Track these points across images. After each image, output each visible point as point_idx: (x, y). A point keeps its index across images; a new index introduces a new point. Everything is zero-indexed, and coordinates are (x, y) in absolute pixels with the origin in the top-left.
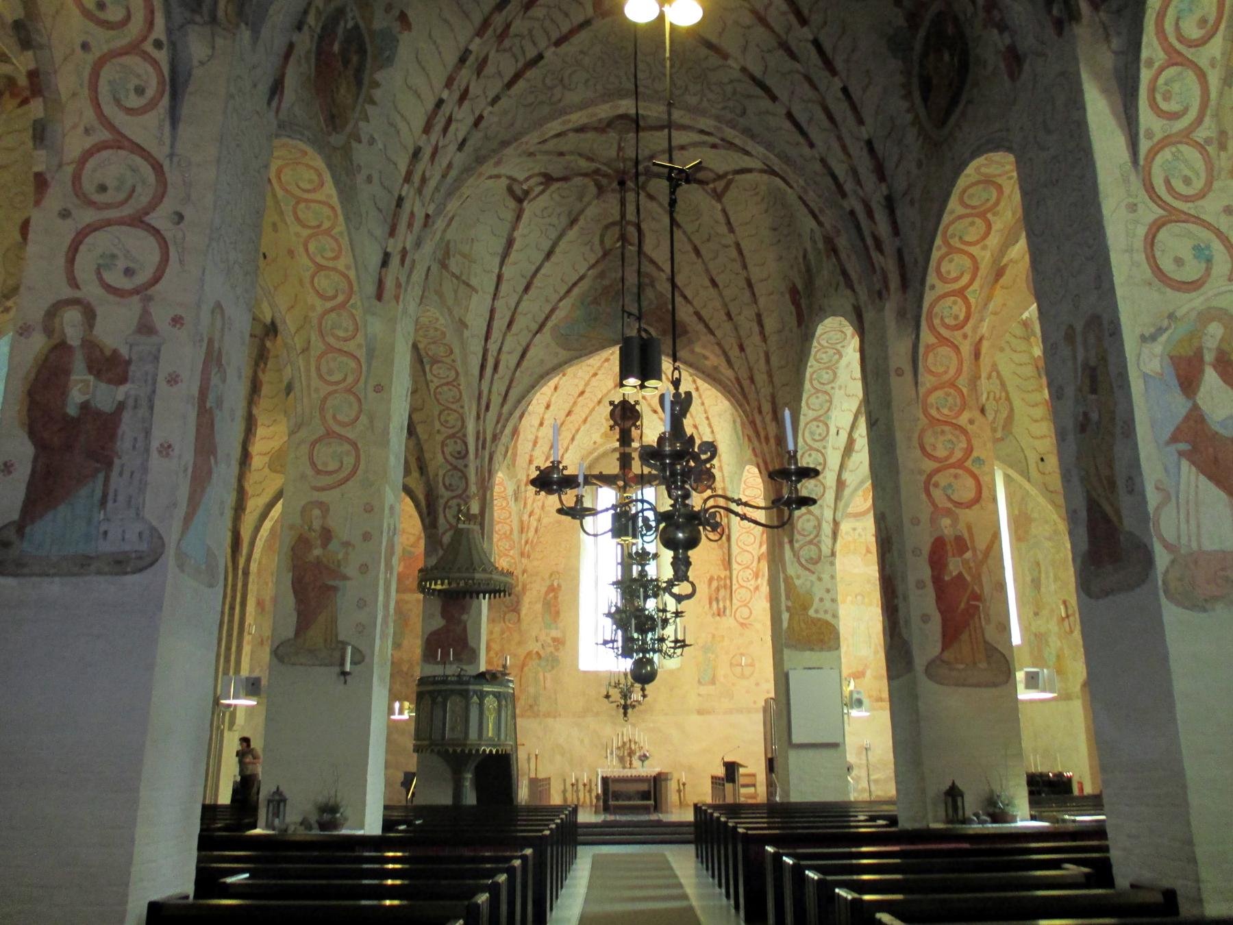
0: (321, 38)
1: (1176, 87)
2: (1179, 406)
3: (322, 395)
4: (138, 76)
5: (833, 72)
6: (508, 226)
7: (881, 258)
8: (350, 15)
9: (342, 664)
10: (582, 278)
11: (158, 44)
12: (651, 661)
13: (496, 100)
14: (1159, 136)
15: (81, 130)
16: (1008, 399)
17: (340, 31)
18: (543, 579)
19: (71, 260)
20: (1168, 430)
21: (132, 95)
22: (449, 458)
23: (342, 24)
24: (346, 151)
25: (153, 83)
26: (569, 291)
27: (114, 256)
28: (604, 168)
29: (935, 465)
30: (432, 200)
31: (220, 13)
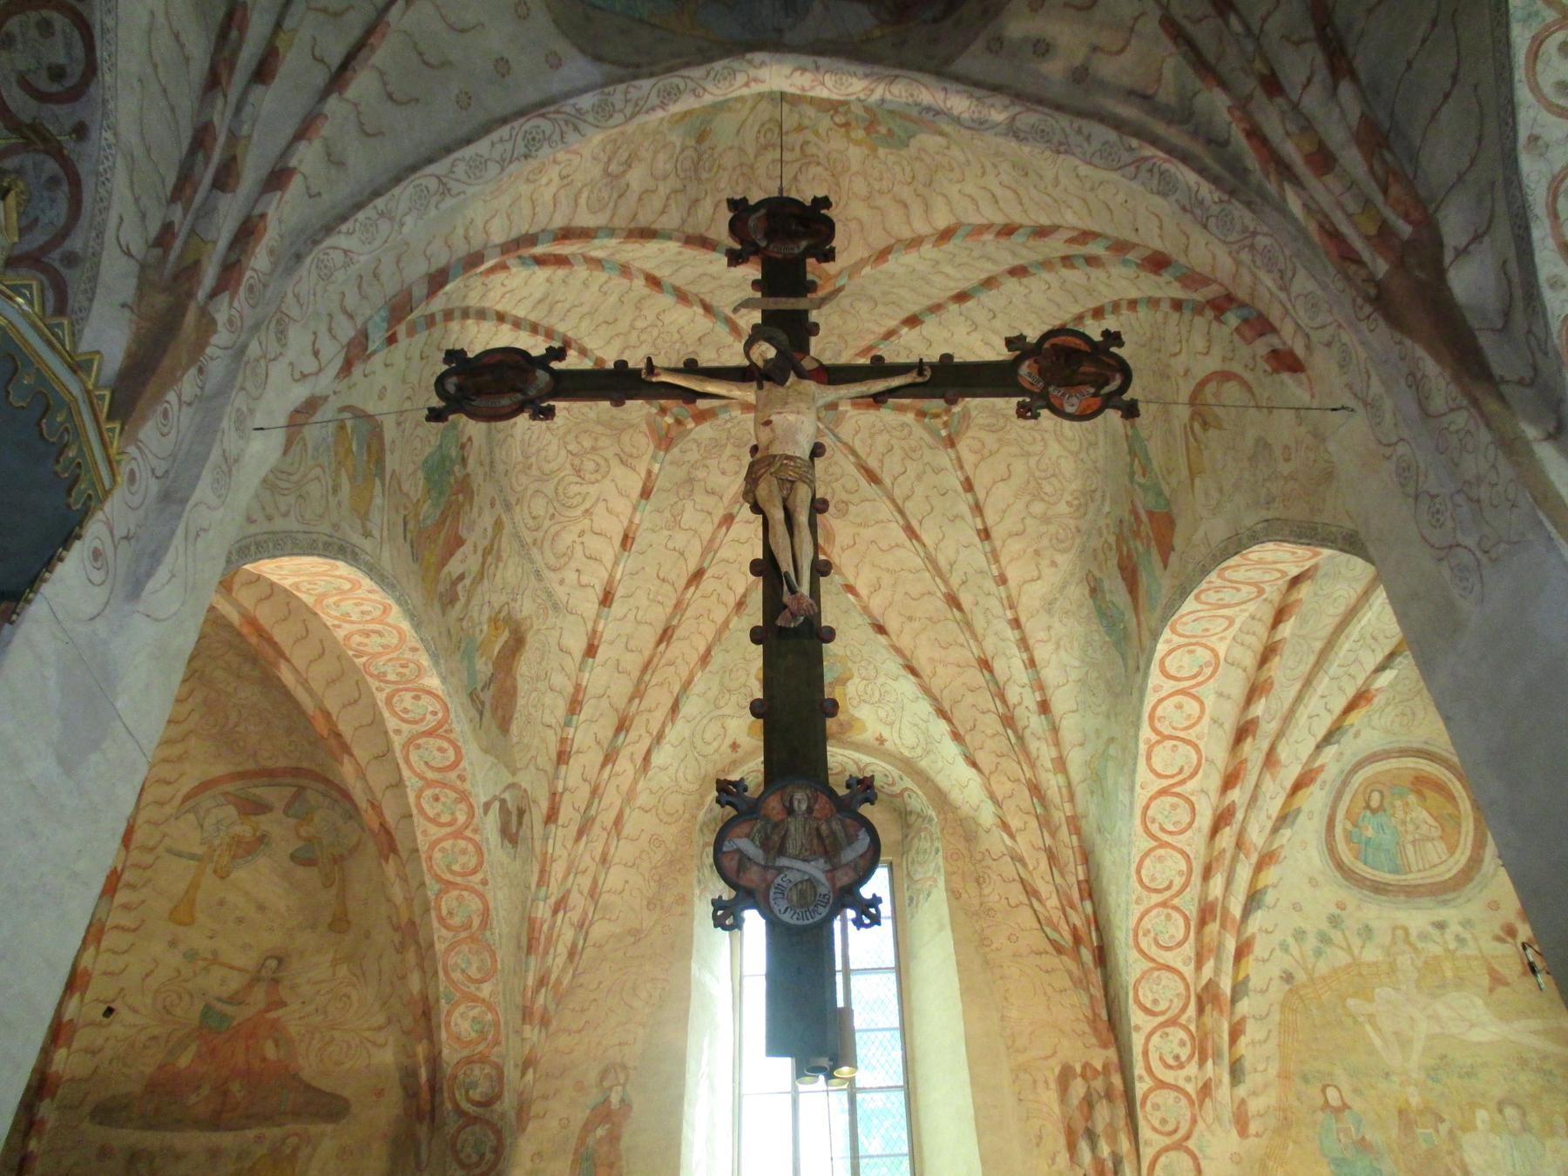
18: (580, 1087)
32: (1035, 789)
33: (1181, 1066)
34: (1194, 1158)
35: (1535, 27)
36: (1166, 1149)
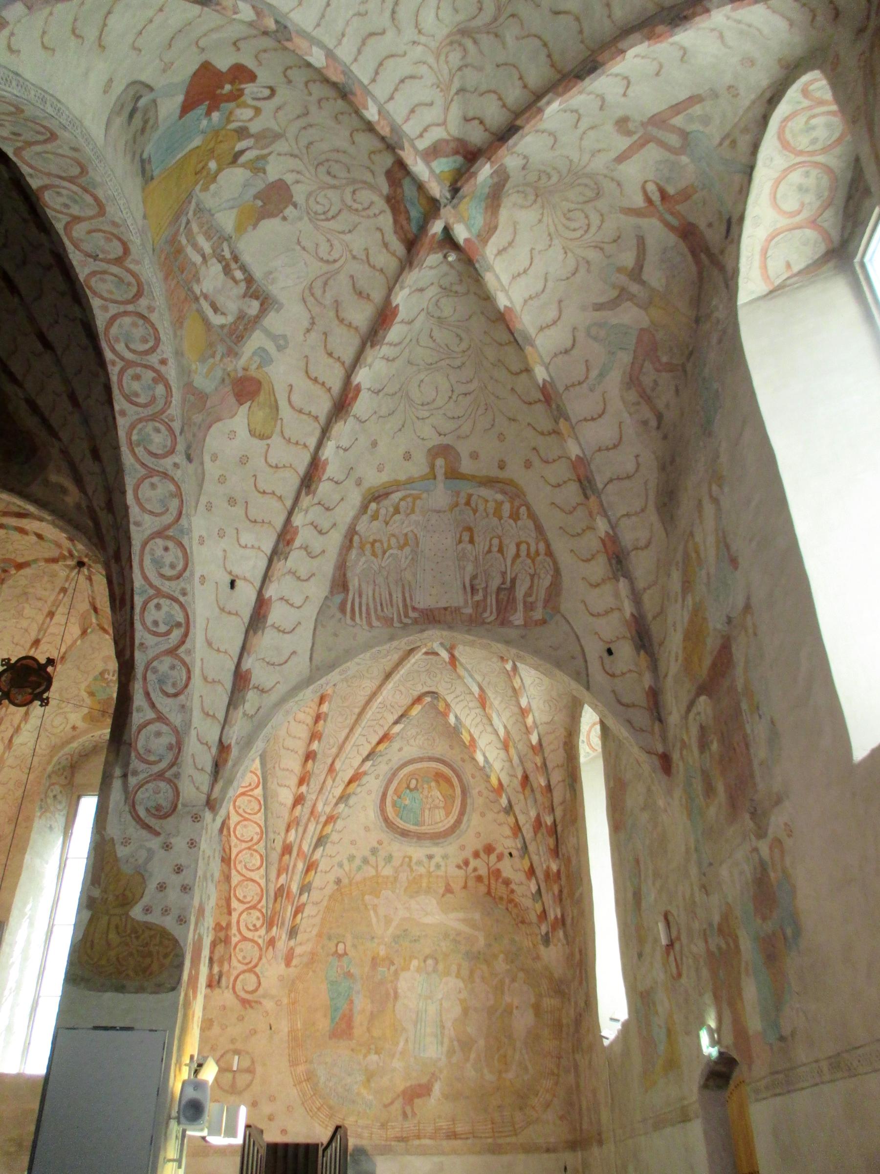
16: (549, 553)
33: (257, 930)
34: (258, 977)
35: (145, 597)
36: (244, 972)
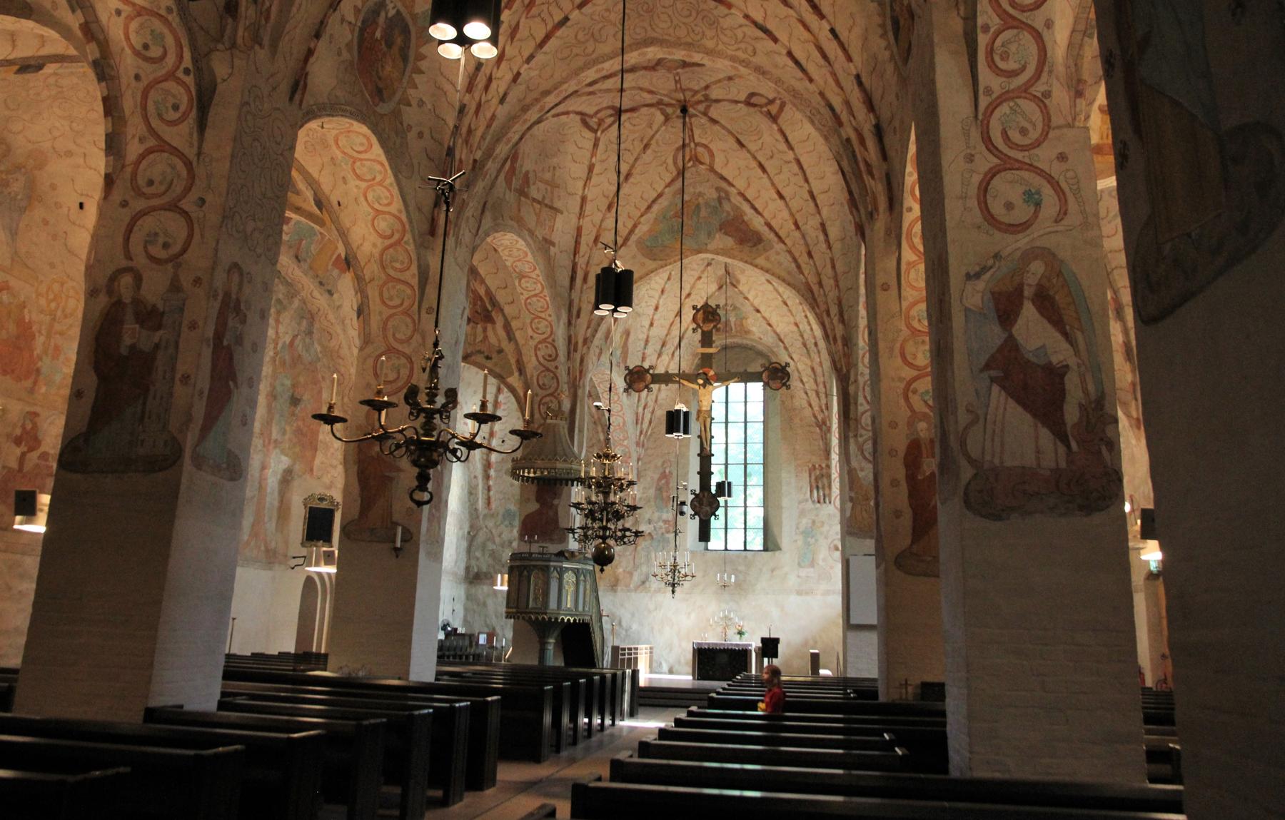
0: (362, 30)
1: (1013, 48)
2: (994, 335)
3: (384, 317)
4: (174, 96)
5: (822, 16)
6: (588, 155)
7: (873, 183)
8: (390, 6)
9: (394, 542)
10: (660, 196)
11: (187, 71)
12: (609, 547)
13: (531, 57)
14: (997, 91)
15: (137, 140)
17: (381, 20)
19: (127, 240)
20: (983, 359)
21: (171, 111)
22: (542, 360)
23: (383, 14)
24: (396, 114)
25: (185, 99)
26: (649, 207)
27: (156, 234)
28: (666, 100)
29: (915, 373)
30: (479, 147)
31: (239, 41)
32: (813, 369)
